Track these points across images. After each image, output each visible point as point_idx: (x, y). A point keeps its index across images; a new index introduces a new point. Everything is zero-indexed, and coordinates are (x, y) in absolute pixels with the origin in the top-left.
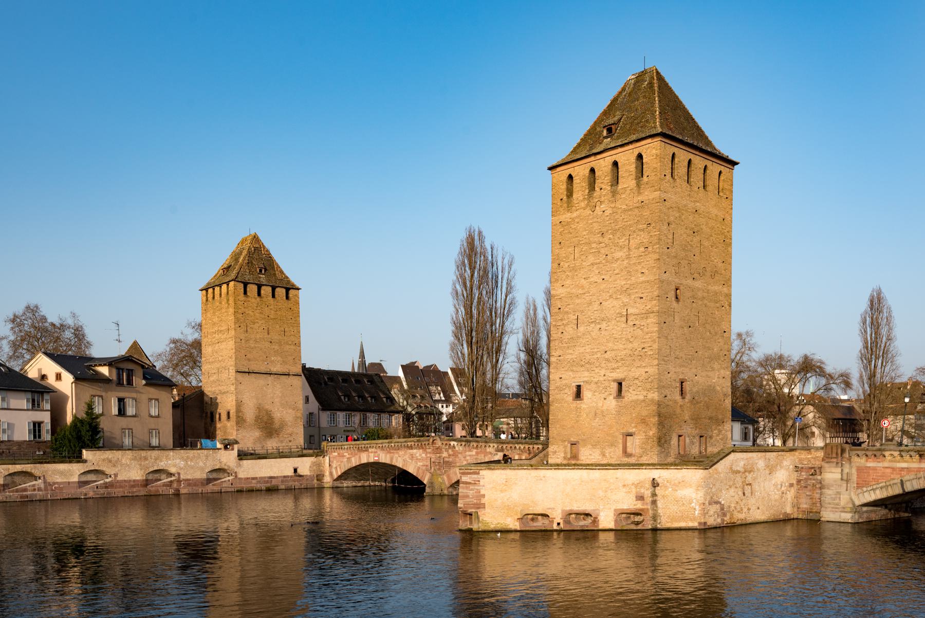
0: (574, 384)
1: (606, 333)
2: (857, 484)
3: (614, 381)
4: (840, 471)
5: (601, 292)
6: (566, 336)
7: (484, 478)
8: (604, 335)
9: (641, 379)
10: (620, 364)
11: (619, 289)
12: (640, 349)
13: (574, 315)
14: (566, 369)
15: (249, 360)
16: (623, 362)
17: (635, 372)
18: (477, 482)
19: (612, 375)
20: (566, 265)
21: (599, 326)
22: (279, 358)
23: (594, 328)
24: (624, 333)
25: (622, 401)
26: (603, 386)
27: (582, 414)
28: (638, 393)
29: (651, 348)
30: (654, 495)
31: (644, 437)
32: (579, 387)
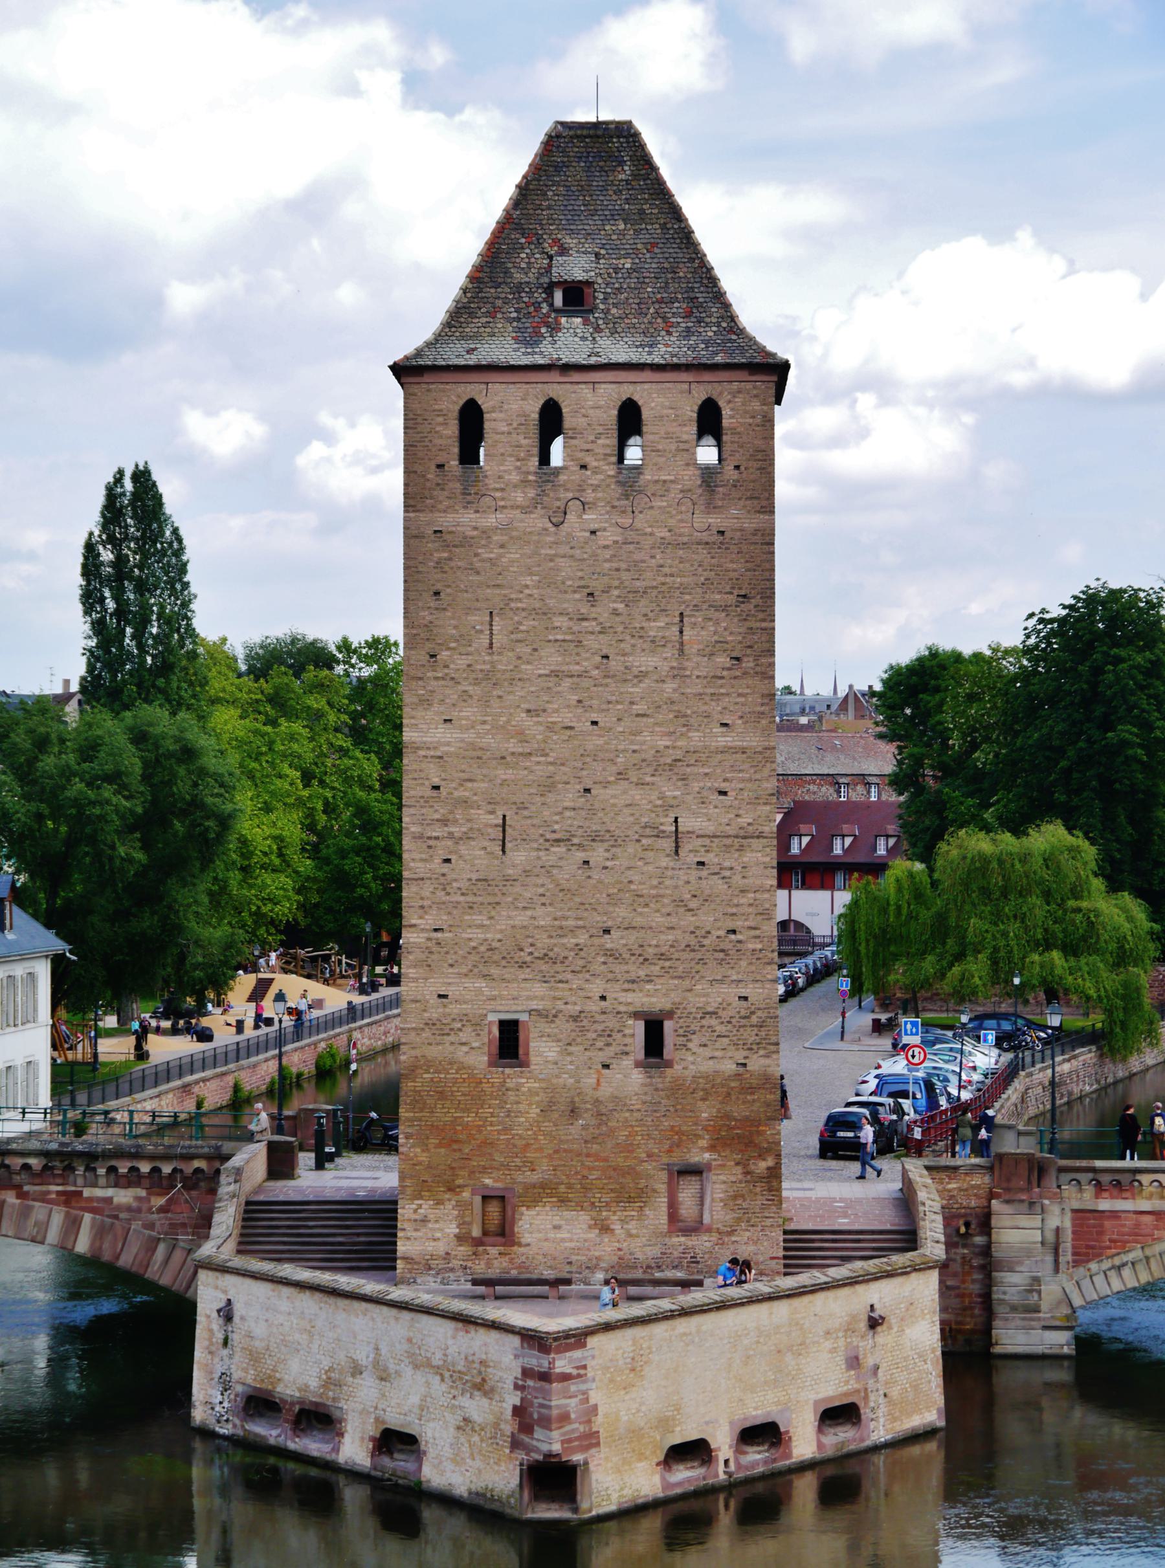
0: (494, 1018)
1: (607, 878)
2: (1074, 1254)
3: (636, 1015)
4: (1040, 1225)
5: (588, 759)
6: (462, 873)
7: (593, 1357)
8: (600, 882)
9: (725, 1015)
10: (658, 968)
11: (649, 755)
12: (722, 933)
13: (492, 812)
14: (464, 970)
16: (667, 964)
17: (707, 995)
18: (582, 1372)
19: (630, 997)
20: (462, 662)
21: (580, 856)
23: (567, 864)
24: (668, 882)
25: (662, 1076)
26: (600, 1027)
27: (522, 1107)
28: (718, 1054)
29: (757, 932)
31: (740, 1177)
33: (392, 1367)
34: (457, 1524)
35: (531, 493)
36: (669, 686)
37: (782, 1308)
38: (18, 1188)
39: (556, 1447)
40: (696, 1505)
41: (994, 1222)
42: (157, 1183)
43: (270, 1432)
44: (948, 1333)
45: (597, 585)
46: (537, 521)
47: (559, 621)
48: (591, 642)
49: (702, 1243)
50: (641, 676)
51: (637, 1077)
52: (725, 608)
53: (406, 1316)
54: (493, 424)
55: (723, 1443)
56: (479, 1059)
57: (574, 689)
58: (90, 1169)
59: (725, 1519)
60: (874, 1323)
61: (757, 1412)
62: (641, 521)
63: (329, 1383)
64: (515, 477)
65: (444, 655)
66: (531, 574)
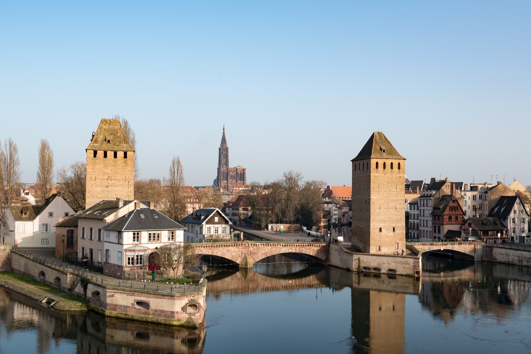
6: (376, 212)
21: (387, 210)
33: (390, 263)
34: (404, 277)
36: (395, 192)
46: (383, 175)
47: (385, 185)
48: (388, 188)
50: (393, 191)
51: (392, 233)
52: (400, 184)
53: (393, 258)
54: (379, 164)
58: (313, 245)
62: (393, 175)
65: (374, 189)
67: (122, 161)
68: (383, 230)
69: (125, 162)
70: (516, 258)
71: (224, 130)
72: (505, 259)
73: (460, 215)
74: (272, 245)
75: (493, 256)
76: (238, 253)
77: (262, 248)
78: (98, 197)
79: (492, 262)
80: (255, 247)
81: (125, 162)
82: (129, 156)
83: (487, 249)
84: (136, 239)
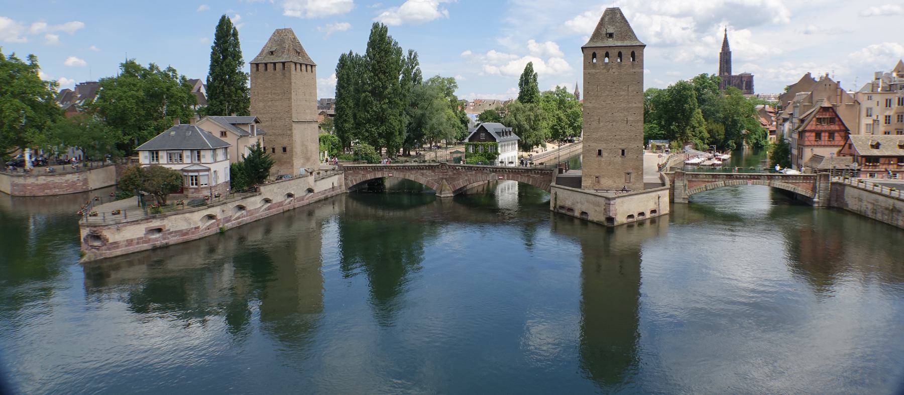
0: (597, 149)
3: (620, 149)
15: (298, 113)
20: (593, 94)
22: (309, 111)
30: (659, 201)
32: (600, 151)
35: (604, 66)
36: (626, 97)
37: (645, 195)
38: (520, 174)
39: (611, 215)
40: (632, 224)
41: (675, 182)
42: (541, 174)
43: (563, 211)
44: (670, 199)
45: (614, 81)
46: (605, 71)
49: (630, 184)
50: (622, 95)
51: (620, 158)
52: (635, 84)
53: (586, 195)
55: (636, 215)
56: (595, 156)
57: (611, 97)
59: (636, 225)
60: (659, 197)
61: (641, 211)
63: (573, 204)
64: (601, 64)
65: (590, 92)
66: (603, 79)
67: (280, 73)
68: (604, 154)
69: (284, 74)
70: (870, 206)
71: (726, 31)
72: (857, 207)
73: (840, 131)
74: (476, 169)
75: (844, 199)
76: (434, 178)
77: (464, 173)
78: (260, 113)
79: (842, 209)
80: (455, 172)
81: (284, 74)
82: (287, 67)
83: (839, 188)
84: (155, 159)
